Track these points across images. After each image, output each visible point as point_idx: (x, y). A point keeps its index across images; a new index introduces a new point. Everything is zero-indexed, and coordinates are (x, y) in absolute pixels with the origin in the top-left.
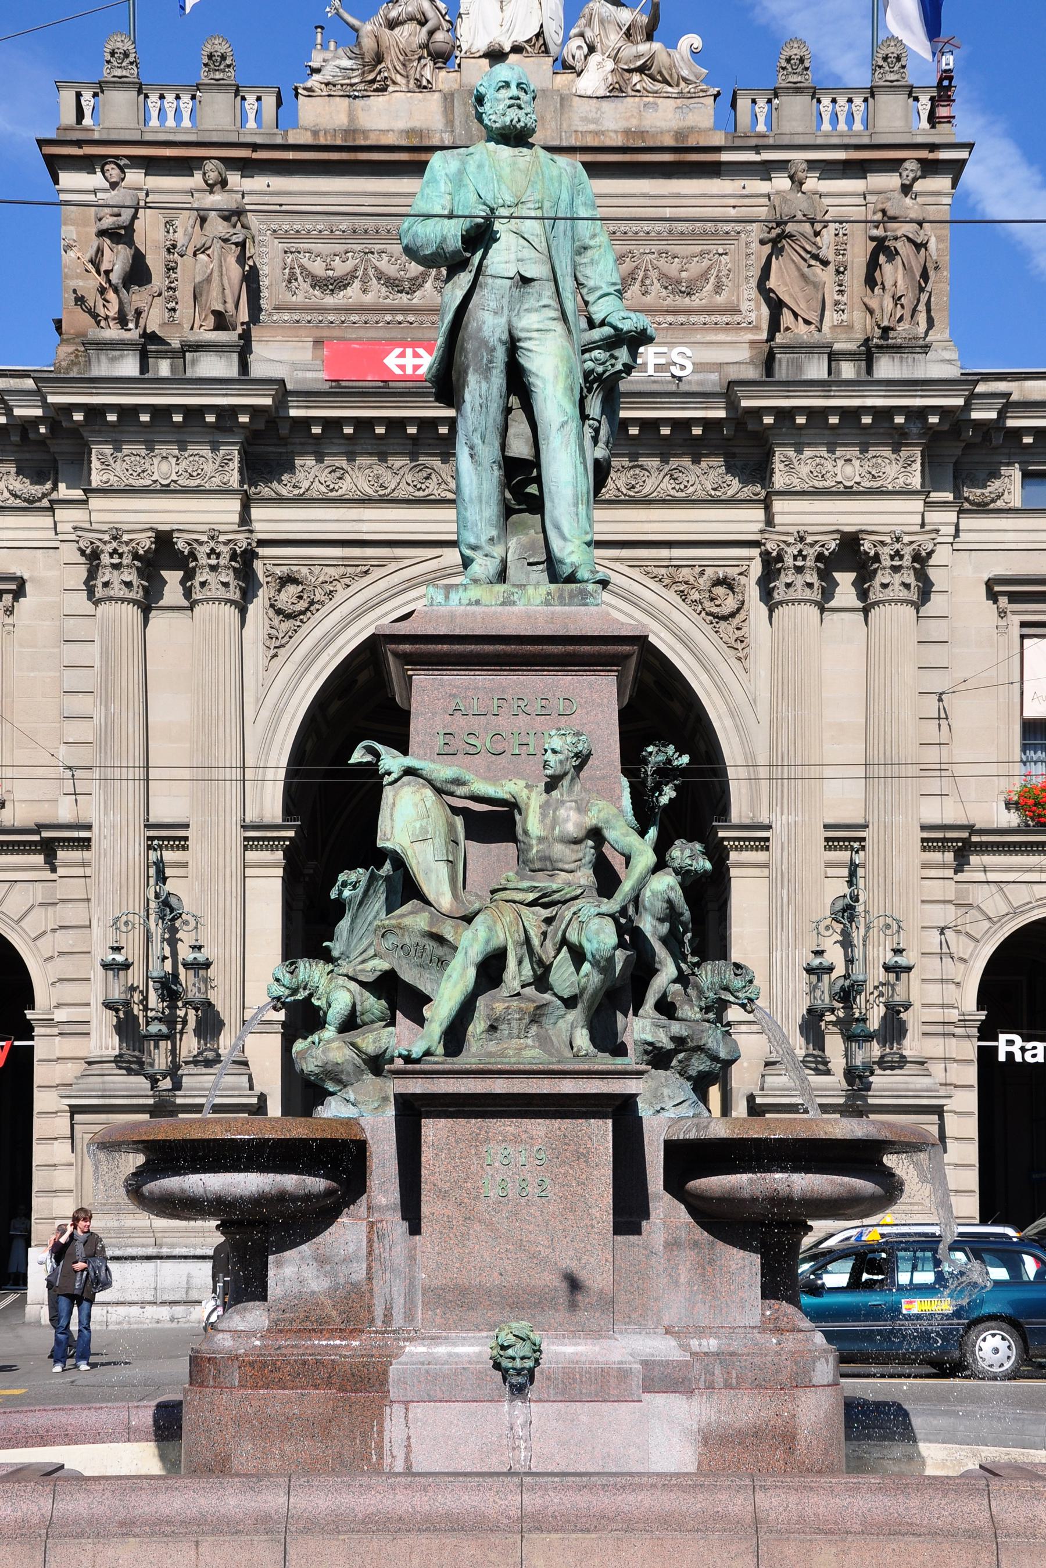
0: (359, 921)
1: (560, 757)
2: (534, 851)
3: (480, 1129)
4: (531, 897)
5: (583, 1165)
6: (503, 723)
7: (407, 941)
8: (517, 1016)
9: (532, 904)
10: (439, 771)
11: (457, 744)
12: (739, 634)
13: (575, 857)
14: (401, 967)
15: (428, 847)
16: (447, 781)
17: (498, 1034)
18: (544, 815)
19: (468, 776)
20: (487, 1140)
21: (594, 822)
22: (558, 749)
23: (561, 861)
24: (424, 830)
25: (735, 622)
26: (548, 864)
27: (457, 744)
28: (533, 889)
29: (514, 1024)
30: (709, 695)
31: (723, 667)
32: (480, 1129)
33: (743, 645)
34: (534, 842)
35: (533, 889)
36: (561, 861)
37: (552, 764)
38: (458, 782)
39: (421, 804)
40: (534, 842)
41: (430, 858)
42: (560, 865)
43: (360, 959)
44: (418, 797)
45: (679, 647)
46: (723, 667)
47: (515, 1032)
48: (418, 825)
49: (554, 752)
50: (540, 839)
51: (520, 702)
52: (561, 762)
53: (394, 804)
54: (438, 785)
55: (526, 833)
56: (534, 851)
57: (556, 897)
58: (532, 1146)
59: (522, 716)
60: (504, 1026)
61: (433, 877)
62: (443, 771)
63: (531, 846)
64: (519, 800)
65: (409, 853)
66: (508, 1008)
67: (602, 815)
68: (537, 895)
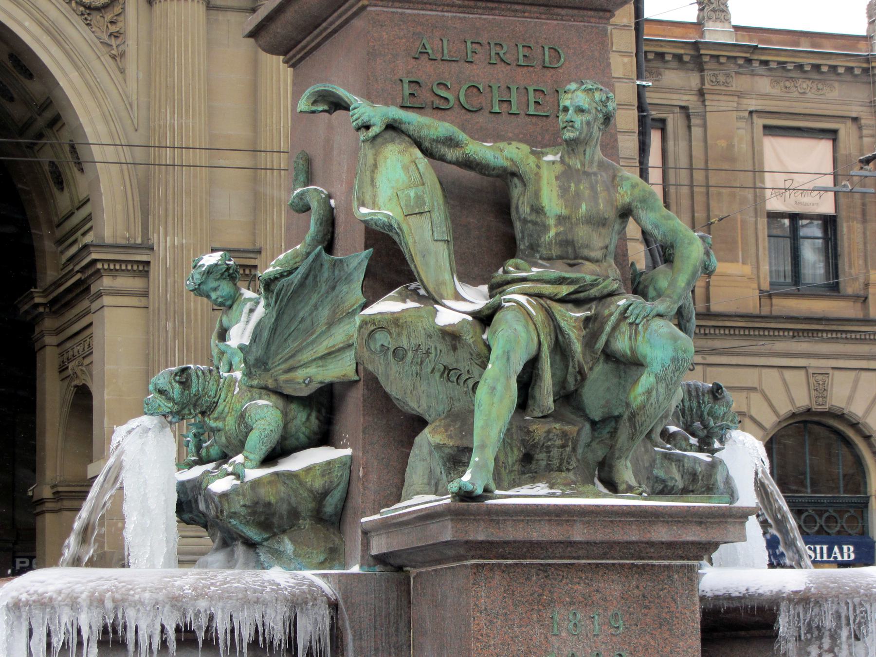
0: (286, 318)
1: (586, 117)
2: (552, 233)
3: (543, 587)
4: (564, 290)
5: (666, 635)
6: (480, 73)
7: (404, 343)
8: (559, 442)
9: (563, 301)
10: (429, 127)
11: (425, 96)
12: (113, 29)
13: (601, 245)
14: (387, 376)
15: (424, 222)
16: (437, 141)
17: (533, 466)
18: (564, 191)
19: (462, 136)
20: (551, 602)
21: (627, 199)
22: (586, 106)
23: (587, 246)
24: (419, 199)
25: (109, 16)
26: (570, 250)
27: (425, 96)
28: (561, 281)
29: (555, 452)
30: (79, 95)
31: (96, 65)
32: (543, 587)
33: (119, 41)
34: (552, 222)
35: (561, 281)
36: (587, 246)
37: (577, 125)
38: (451, 142)
39: (412, 167)
40: (552, 222)
41: (428, 235)
42: (585, 252)
43: (284, 366)
44: (407, 159)
45: (45, 39)
46: (96, 65)
47: (556, 463)
48: (412, 194)
49: (580, 110)
50: (561, 219)
51: (498, 49)
52: (588, 123)
53: (375, 166)
54: (427, 144)
55: (538, 210)
56: (552, 233)
57: (594, 292)
58: (605, 610)
59: (501, 67)
60: (543, 456)
61: (432, 261)
62: (436, 127)
63: (546, 228)
64: (523, 169)
65: (405, 228)
66: (549, 432)
67: (636, 191)
68: (572, 288)
